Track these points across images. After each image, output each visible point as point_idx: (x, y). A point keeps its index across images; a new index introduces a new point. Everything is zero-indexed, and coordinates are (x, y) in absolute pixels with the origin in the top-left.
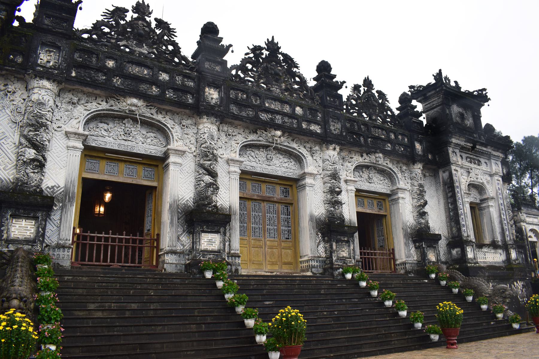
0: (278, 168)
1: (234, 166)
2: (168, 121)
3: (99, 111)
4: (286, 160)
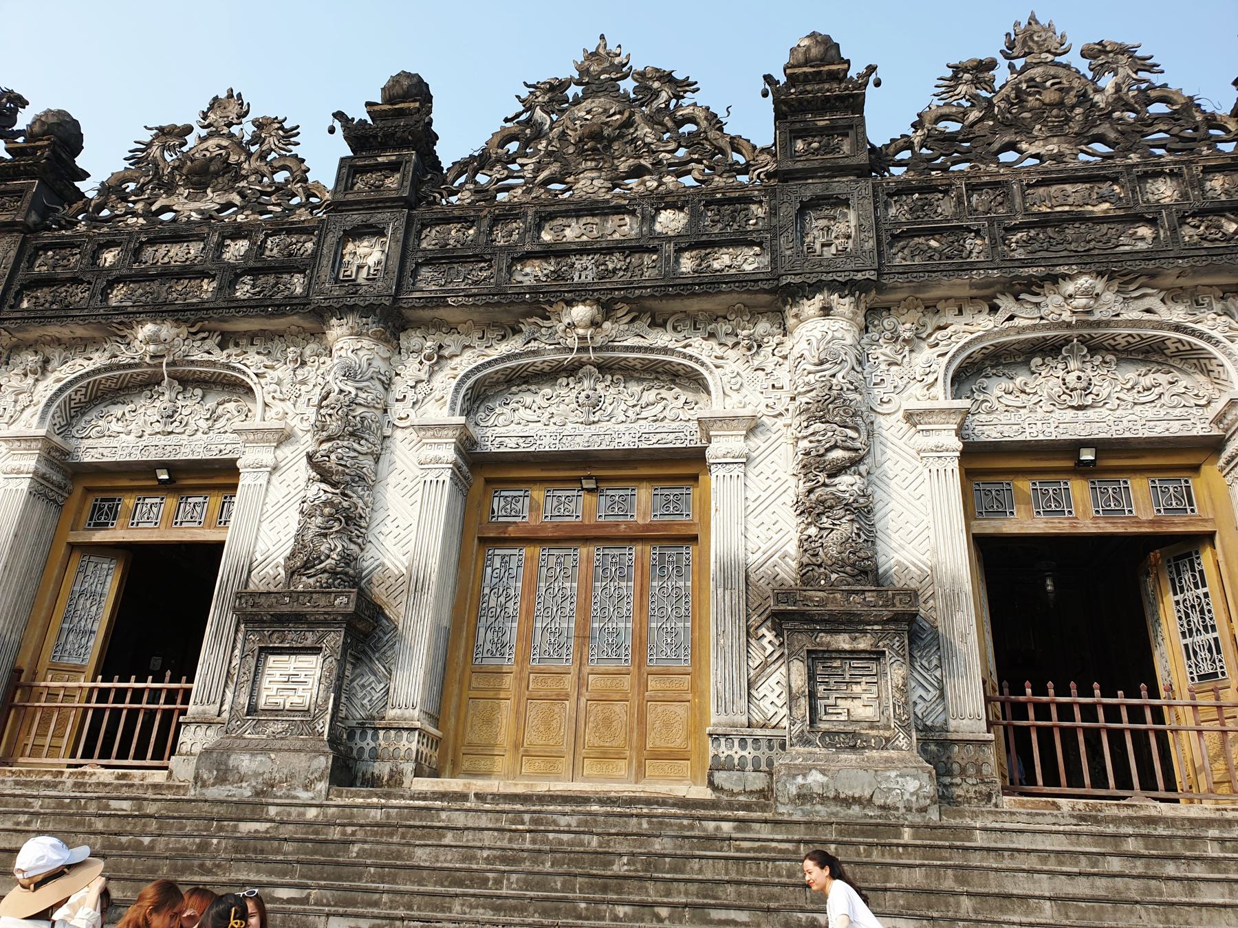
0: (622, 427)
1: (439, 444)
2: (250, 362)
3: (88, 374)
4: (650, 396)
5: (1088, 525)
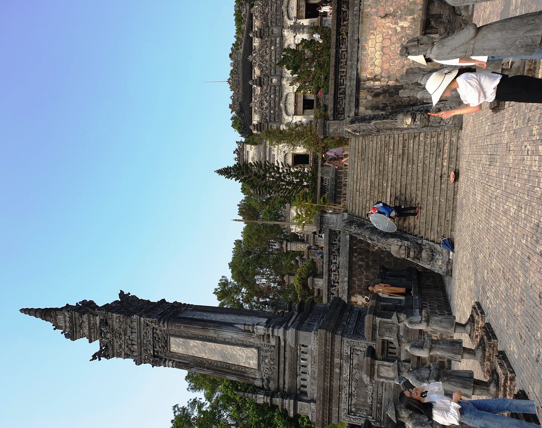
2: (285, 94)
5: (305, 8)
